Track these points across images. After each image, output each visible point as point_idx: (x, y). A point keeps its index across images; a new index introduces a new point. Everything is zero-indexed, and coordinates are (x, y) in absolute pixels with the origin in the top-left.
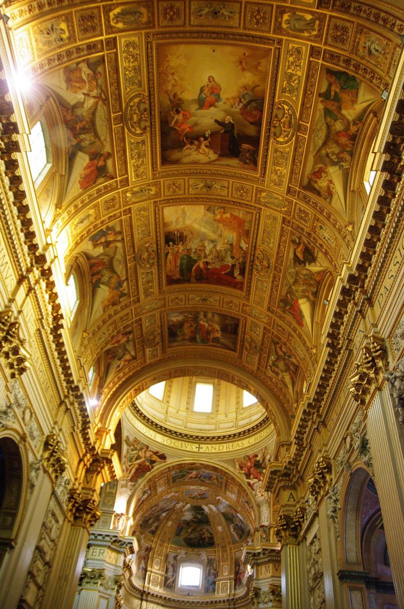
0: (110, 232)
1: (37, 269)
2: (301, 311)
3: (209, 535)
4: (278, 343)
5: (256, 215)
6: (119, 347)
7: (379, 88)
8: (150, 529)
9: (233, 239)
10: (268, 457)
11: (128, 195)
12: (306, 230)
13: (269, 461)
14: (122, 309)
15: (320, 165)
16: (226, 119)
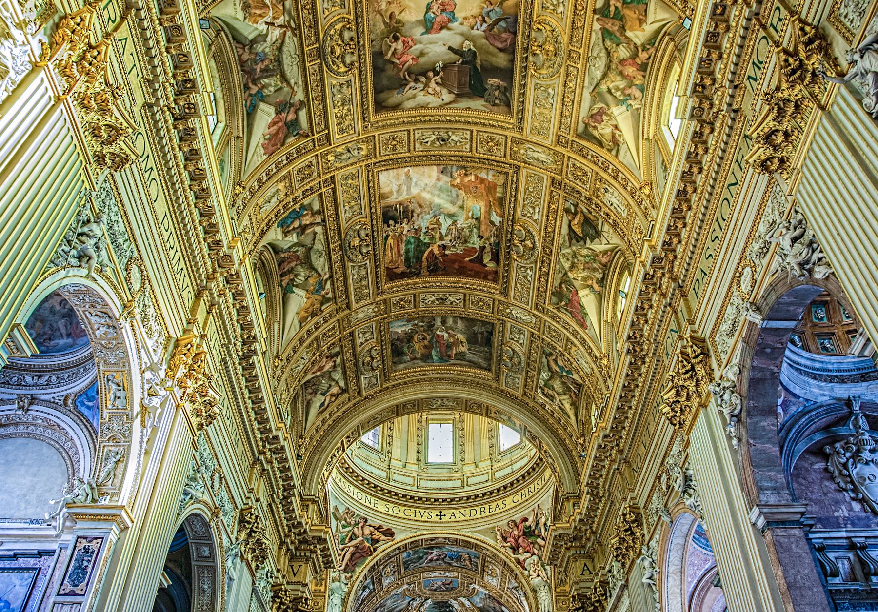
0: (305, 212)
1: (222, 275)
2: (582, 307)
4: (551, 354)
5: (512, 177)
6: (322, 376)
7: (675, 5)
9: (480, 210)
10: (543, 520)
11: (331, 158)
12: (585, 193)
13: (545, 524)
14: (325, 321)
15: (600, 105)
16: (464, 45)
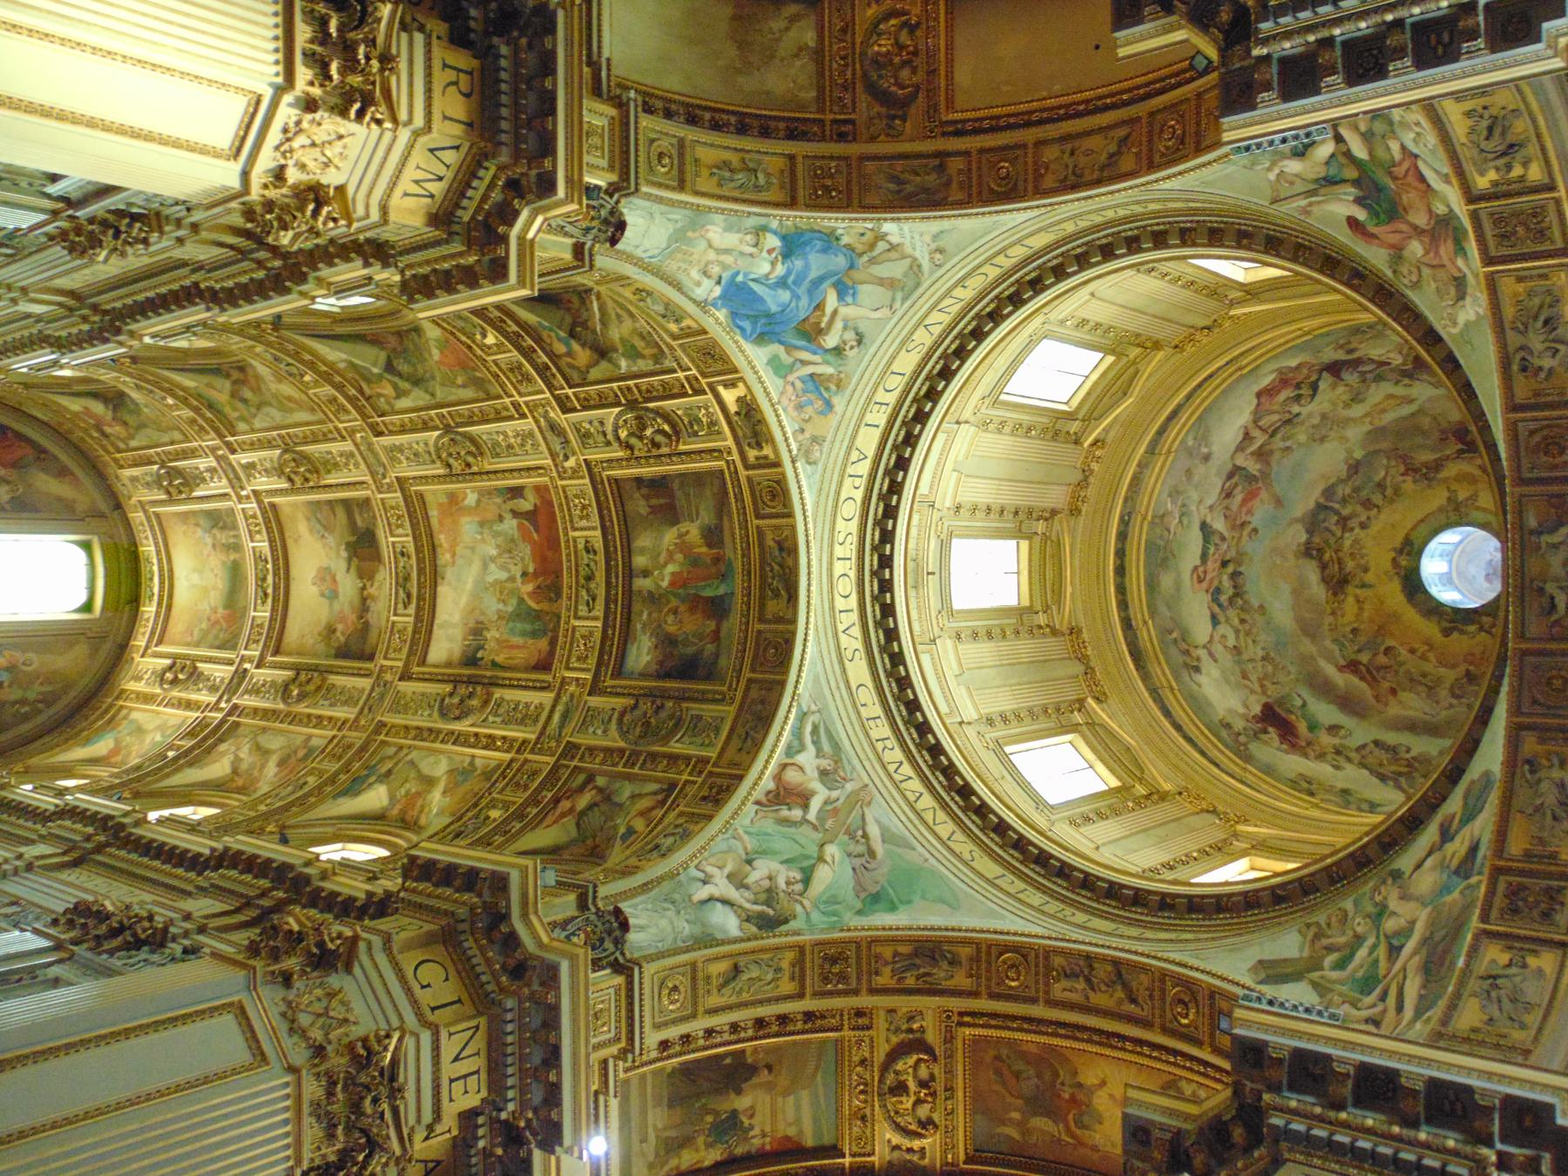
10: (1294, 166)
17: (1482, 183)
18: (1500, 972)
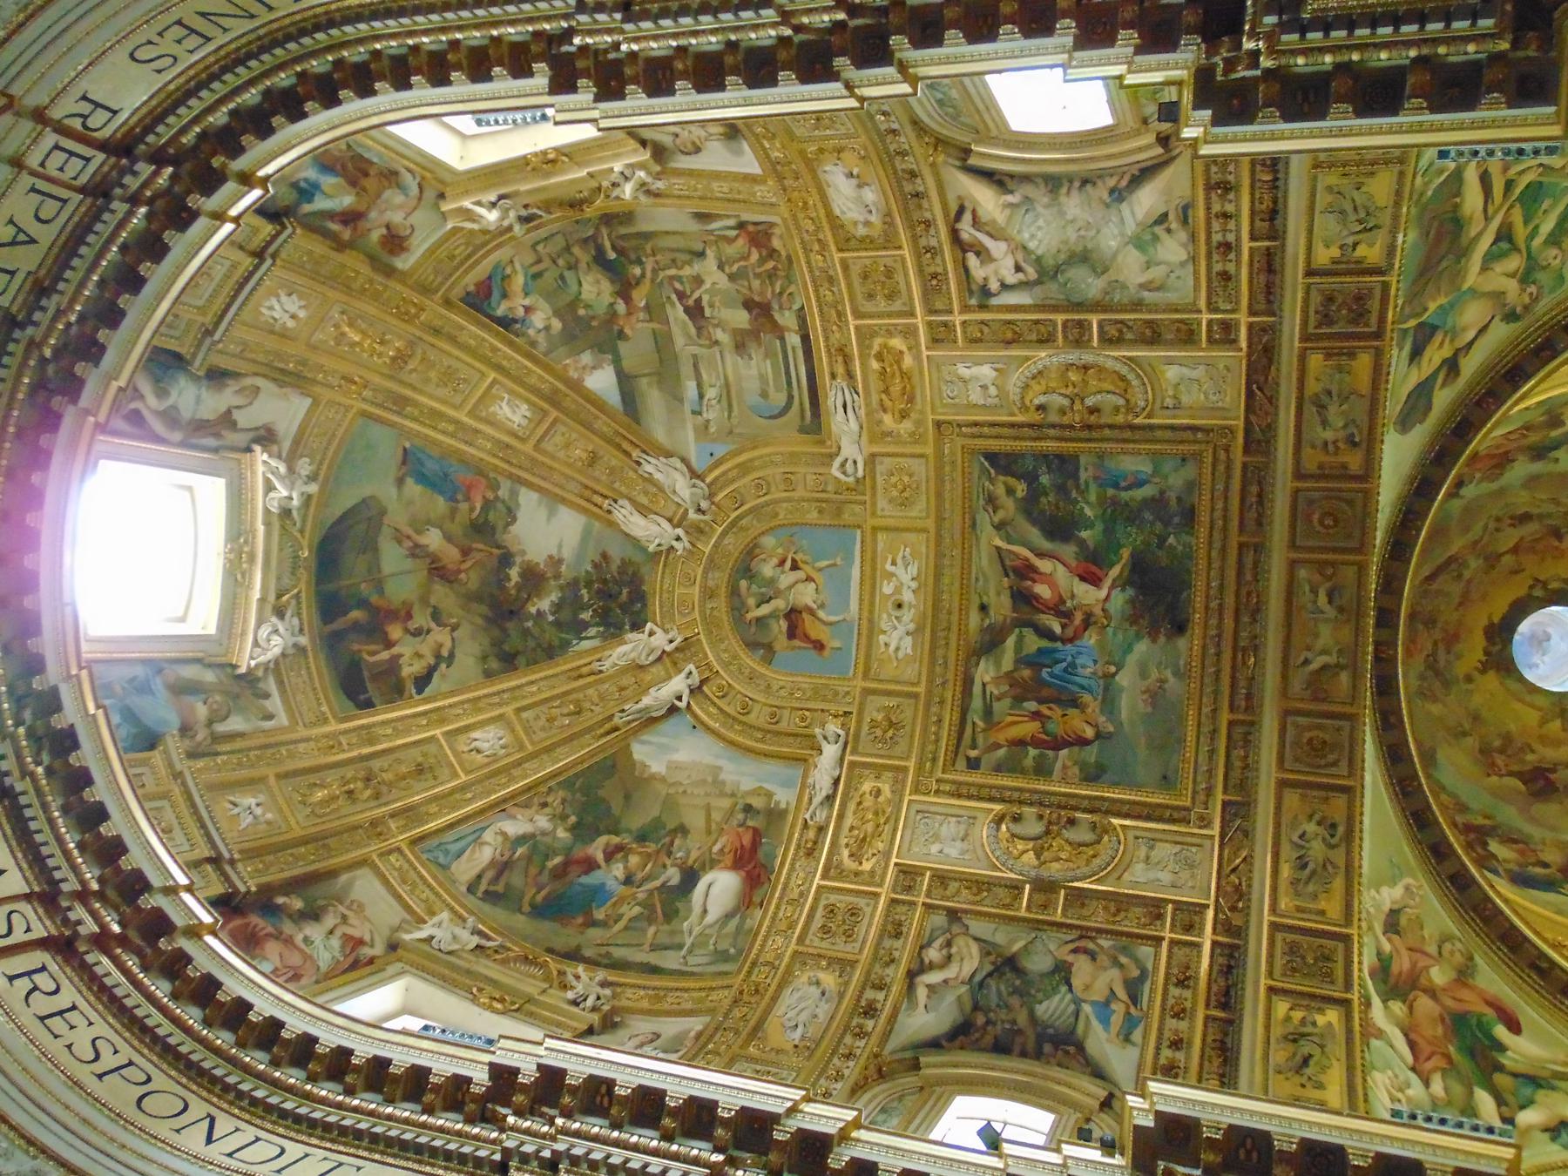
3: (410, 669)
8: (519, 280)
17: (1332, 1016)
18: (1361, 236)
